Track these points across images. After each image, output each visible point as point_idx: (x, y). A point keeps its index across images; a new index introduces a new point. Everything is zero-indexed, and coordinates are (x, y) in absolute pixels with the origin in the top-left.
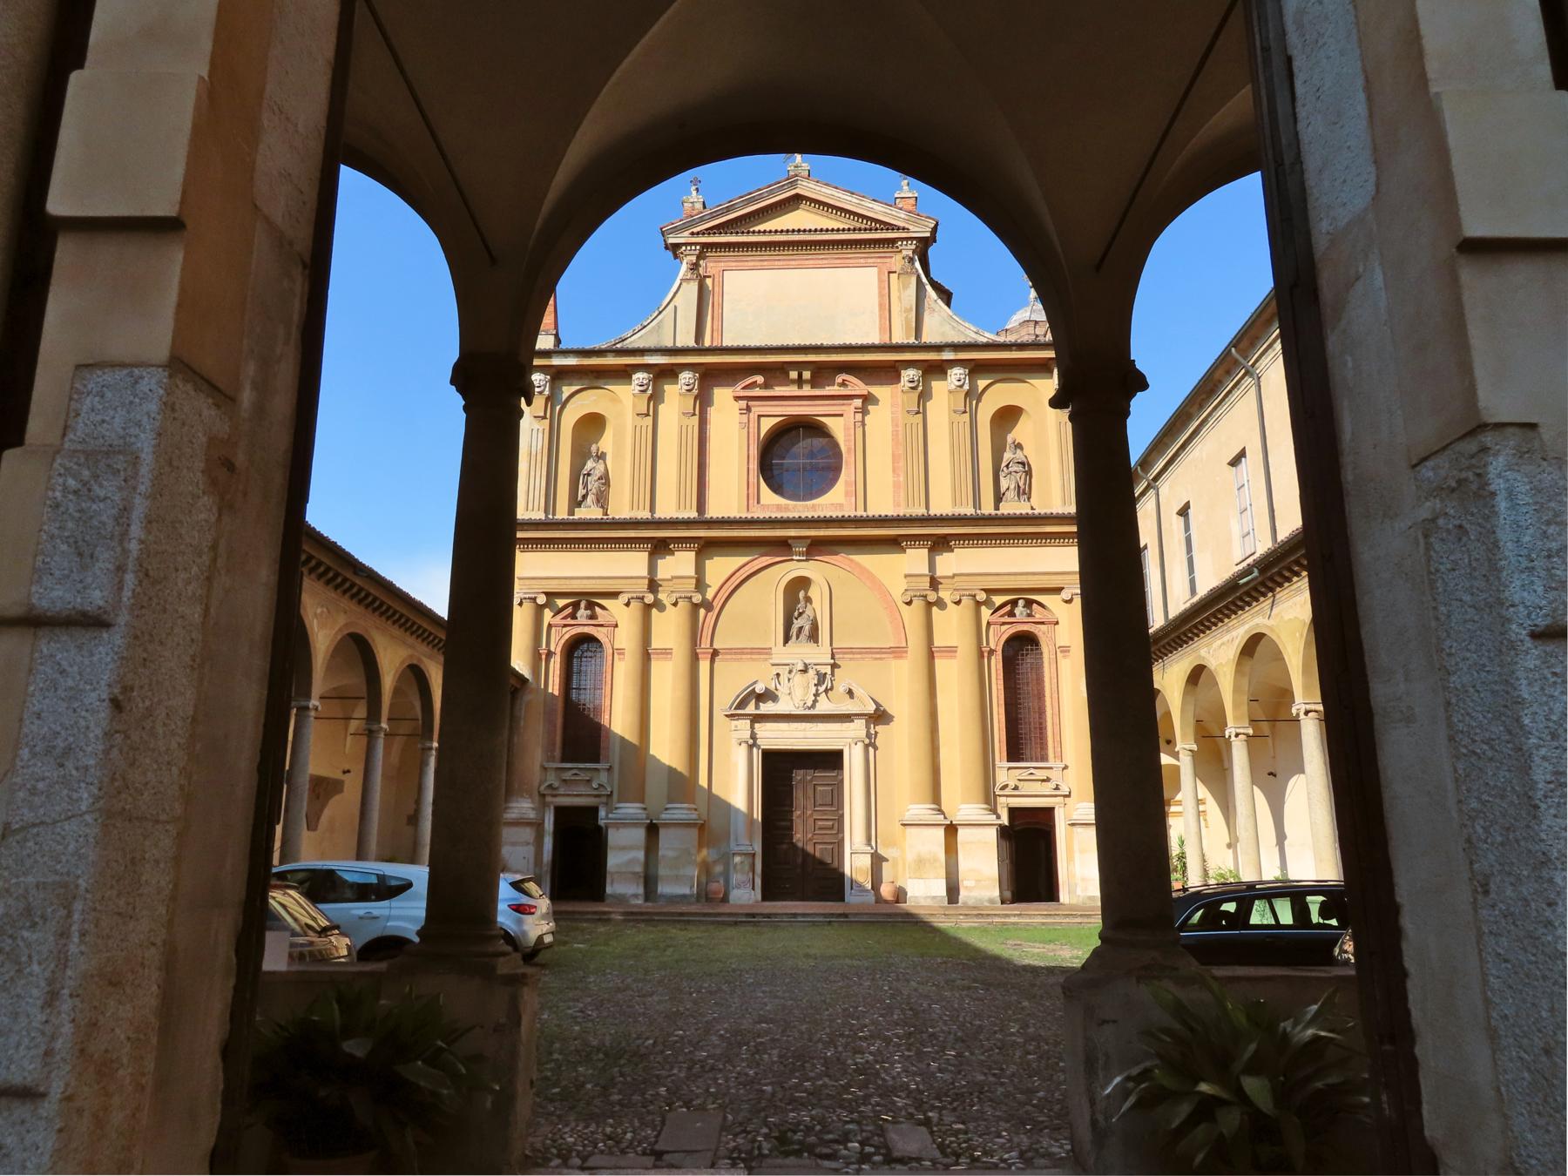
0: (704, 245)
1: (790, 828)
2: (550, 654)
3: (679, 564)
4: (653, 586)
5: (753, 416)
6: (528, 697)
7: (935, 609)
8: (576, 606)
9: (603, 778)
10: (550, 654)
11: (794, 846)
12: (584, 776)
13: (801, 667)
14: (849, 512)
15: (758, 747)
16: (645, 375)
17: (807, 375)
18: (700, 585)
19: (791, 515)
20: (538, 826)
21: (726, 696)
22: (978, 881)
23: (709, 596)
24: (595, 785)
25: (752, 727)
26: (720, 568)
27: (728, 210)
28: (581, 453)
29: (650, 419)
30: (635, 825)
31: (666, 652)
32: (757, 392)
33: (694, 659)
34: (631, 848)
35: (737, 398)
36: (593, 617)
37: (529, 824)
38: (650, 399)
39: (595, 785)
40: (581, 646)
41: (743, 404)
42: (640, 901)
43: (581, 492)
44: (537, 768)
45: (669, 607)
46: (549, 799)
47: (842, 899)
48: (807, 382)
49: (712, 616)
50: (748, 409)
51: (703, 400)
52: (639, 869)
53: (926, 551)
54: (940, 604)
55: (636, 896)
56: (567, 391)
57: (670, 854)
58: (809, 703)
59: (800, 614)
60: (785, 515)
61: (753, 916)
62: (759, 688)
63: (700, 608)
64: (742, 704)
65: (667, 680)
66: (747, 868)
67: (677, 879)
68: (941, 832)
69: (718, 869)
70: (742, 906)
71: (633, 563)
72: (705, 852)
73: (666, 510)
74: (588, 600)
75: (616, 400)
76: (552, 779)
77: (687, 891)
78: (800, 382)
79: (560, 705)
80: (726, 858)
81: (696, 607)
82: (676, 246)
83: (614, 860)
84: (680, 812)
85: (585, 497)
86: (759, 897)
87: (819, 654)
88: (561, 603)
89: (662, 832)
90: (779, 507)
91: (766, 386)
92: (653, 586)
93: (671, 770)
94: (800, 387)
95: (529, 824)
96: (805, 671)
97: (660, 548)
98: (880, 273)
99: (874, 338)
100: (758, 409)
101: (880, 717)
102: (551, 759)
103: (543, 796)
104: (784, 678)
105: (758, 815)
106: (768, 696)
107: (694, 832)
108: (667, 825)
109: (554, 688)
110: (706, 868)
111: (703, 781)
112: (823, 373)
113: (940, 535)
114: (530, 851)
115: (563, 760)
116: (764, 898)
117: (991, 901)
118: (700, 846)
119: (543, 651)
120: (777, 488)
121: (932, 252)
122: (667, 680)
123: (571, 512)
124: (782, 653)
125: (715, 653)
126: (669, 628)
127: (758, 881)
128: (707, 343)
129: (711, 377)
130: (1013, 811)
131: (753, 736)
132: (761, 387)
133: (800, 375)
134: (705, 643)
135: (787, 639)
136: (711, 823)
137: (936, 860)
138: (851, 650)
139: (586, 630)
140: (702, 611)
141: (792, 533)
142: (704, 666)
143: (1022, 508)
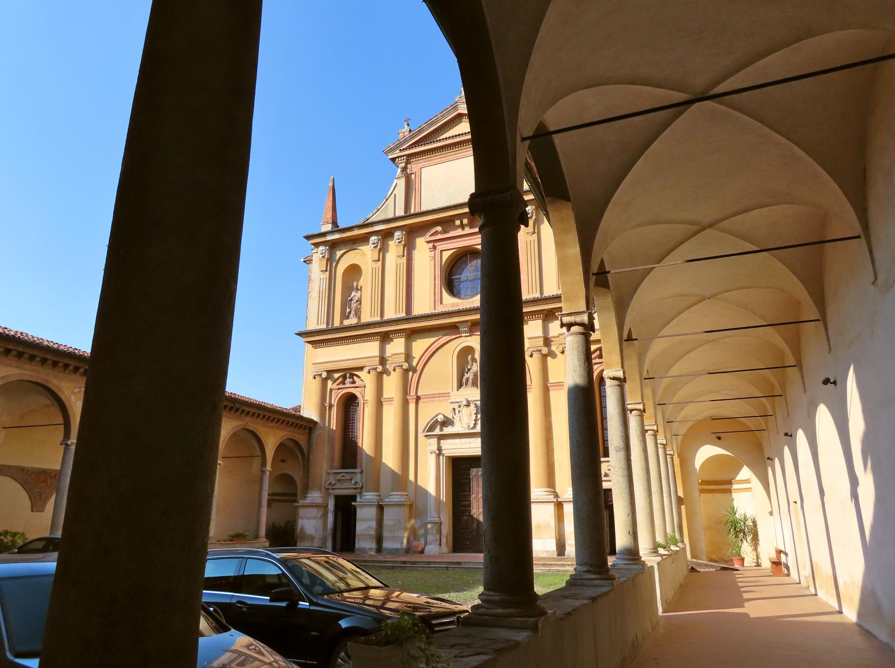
1: (469, 506)
2: (331, 406)
3: (397, 346)
4: (383, 360)
5: (438, 252)
6: (317, 432)
7: (549, 359)
8: (344, 377)
9: (358, 478)
10: (331, 406)
11: (472, 517)
12: (348, 477)
13: (465, 403)
15: (443, 455)
16: (376, 237)
17: (465, 221)
18: (408, 357)
20: (326, 507)
21: (423, 423)
23: (414, 364)
24: (353, 482)
25: (439, 443)
26: (420, 346)
27: (420, 132)
28: (348, 288)
29: (380, 262)
30: (370, 506)
31: (390, 400)
32: (439, 237)
33: (405, 403)
35: (428, 242)
36: (354, 382)
37: (317, 506)
38: (380, 250)
39: (353, 482)
40: (350, 402)
41: (431, 245)
42: (373, 553)
43: (348, 310)
44: (324, 473)
45: (392, 372)
46: (330, 491)
48: (466, 225)
49: (416, 376)
50: (434, 248)
51: (409, 247)
52: (373, 532)
54: (552, 354)
55: (371, 549)
56: (339, 253)
58: (472, 426)
59: (469, 370)
62: (440, 418)
63: (409, 371)
64: (431, 428)
65: (391, 415)
69: (422, 532)
71: (371, 349)
72: (413, 521)
73: (389, 314)
74: (349, 373)
75: (364, 254)
78: (462, 226)
79: (338, 438)
80: (425, 525)
81: (406, 371)
82: (393, 160)
83: (360, 527)
85: (350, 313)
86: (445, 549)
88: (336, 376)
89: (386, 509)
90: (453, 305)
91: (445, 231)
92: (383, 360)
93: (393, 471)
94: (463, 229)
95: (317, 506)
96: (468, 405)
97: (385, 338)
100: (440, 246)
102: (332, 467)
104: (457, 412)
105: (443, 497)
106: (447, 422)
107: (407, 510)
109: (334, 423)
110: (414, 533)
111: (412, 477)
115: (343, 467)
118: (410, 517)
119: (327, 405)
122: (391, 415)
123: (341, 322)
125: (418, 399)
126: (392, 385)
128: (412, 212)
129: (413, 232)
131: (440, 449)
132: (441, 233)
133: (462, 222)
134: (413, 393)
135: (460, 386)
136: (416, 503)
140: (411, 373)
141: (456, 319)
142: (412, 406)
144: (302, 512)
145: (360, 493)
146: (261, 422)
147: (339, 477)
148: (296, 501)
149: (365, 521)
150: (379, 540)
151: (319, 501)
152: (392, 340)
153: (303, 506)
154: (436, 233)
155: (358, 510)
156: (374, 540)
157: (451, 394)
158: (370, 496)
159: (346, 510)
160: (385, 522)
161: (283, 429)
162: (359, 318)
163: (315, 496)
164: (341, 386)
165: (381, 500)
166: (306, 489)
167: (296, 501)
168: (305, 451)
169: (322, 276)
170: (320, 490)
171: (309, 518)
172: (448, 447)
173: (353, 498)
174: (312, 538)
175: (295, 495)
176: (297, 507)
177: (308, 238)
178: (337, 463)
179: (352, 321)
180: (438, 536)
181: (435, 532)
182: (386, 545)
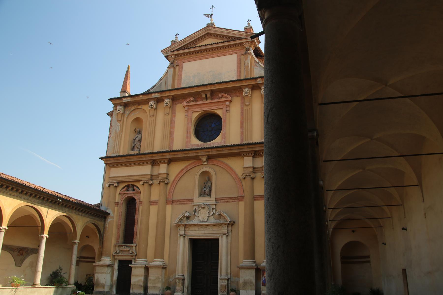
0: (176, 55)
12: (128, 249)
14: (223, 144)
17: (208, 95)
24: (130, 252)
26: (176, 169)
30: (141, 267)
34: (140, 276)
36: (134, 190)
37: (108, 266)
39: (130, 252)
41: (186, 108)
46: (116, 257)
58: (206, 220)
62: (187, 214)
64: (180, 221)
68: (253, 272)
76: (117, 249)
77: (157, 293)
78: (206, 98)
87: (211, 200)
89: (150, 270)
90: (198, 145)
91: (195, 100)
95: (108, 266)
97: (154, 163)
98: (238, 56)
101: (231, 224)
103: (115, 256)
104: (197, 211)
108: (151, 267)
112: (214, 94)
114: (108, 277)
124: (199, 201)
128: (176, 87)
132: (193, 101)
133: (206, 95)
137: (251, 282)
138: (223, 199)
139: (131, 195)
144: (98, 269)
145: (135, 259)
146: (74, 211)
147: (122, 248)
148: (94, 262)
149: (137, 277)
150: (146, 288)
151: (109, 263)
152: (159, 165)
153: (99, 266)
154: (190, 101)
155: (133, 269)
156: (142, 288)
157: (194, 200)
158: (141, 261)
159: (125, 268)
160: (149, 278)
161: (88, 217)
162: (139, 150)
163: (106, 260)
164: (126, 192)
165: (148, 264)
166: (101, 255)
167: (94, 262)
168: (102, 231)
169: (118, 124)
170: (110, 256)
171: (102, 273)
173: (130, 262)
174: (103, 286)
175: (94, 258)
176: (95, 266)
177: (110, 100)
178: (121, 240)
179: (136, 152)
180: (182, 287)
181: (181, 284)
182: (150, 291)
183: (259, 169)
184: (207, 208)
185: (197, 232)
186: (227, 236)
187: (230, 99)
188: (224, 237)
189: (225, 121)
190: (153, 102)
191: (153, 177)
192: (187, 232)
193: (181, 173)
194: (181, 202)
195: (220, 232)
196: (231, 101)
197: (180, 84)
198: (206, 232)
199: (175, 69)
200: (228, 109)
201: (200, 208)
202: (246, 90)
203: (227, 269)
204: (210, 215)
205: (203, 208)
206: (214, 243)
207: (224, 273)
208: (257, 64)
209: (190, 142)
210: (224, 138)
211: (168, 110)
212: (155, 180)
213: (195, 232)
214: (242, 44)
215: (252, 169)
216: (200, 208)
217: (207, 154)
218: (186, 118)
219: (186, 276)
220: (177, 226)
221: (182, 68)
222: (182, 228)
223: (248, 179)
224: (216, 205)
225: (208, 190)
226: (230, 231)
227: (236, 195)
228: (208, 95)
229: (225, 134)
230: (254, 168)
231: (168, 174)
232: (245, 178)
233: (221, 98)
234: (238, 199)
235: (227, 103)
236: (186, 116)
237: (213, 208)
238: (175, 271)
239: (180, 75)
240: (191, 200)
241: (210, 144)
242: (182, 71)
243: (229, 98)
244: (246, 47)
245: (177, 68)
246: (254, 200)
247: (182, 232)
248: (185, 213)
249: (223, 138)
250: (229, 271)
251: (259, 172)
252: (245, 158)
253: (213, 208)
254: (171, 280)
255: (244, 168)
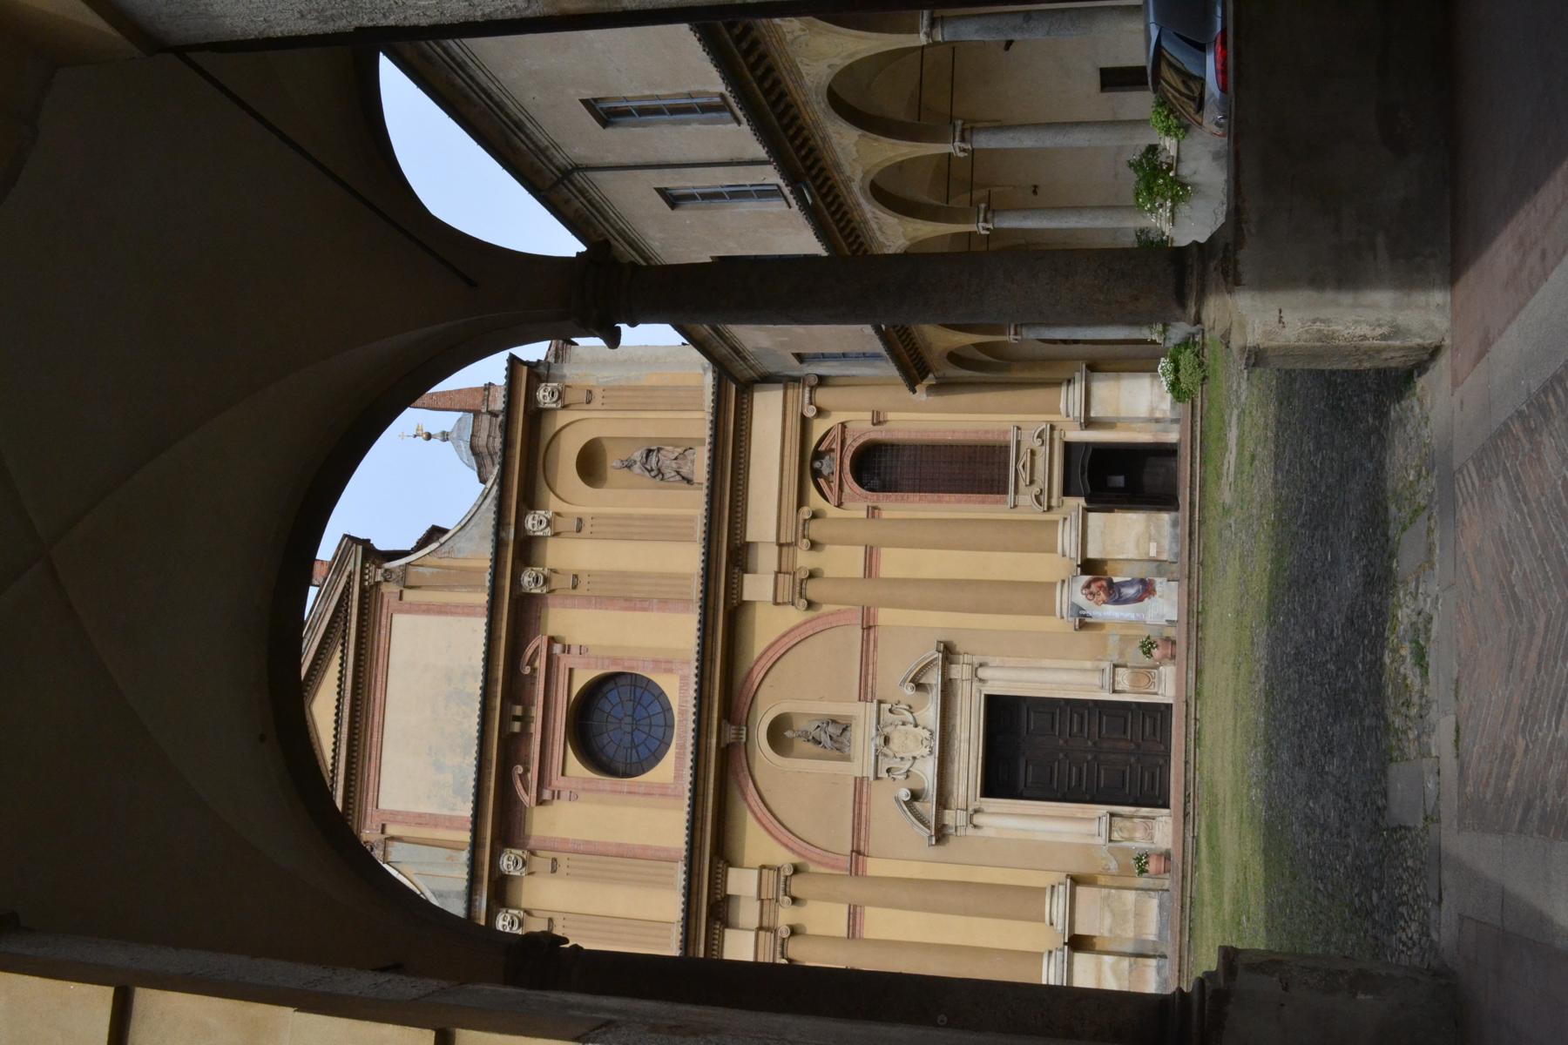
17: (518, 710)
19: (690, 741)
22: (1150, 539)
41: (547, 795)
47: (1169, 707)
52: (1126, 962)
53: (746, 576)
55: (1159, 970)
57: (1108, 921)
58: (927, 734)
60: (690, 749)
61: (1186, 815)
62: (904, 794)
66: (1128, 824)
67: (1139, 915)
70: (1175, 832)
78: (525, 720)
84: (1057, 908)
86: (1165, 811)
87: (863, 716)
89: (1079, 930)
90: (680, 757)
98: (401, 611)
99: (481, 623)
107: (1081, 891)
113: (727, 554)
116: (1166, 806)
117: (1175, 524)
120: (655, 757)
121: (381, 545)
124: (861, 762)
127: (1144, 811)
130: (1067, 491)
132: (526, 770)
133: (517, 718)
135: (847, 759)
143: (702, 457)
154: (523, 777)
157: (859, 775)
172: (962, 790)
183: (784, 559)
184: (887, 730)
185: (963, 765)
186: (981, 665)
187: (545, 639)
188: (982, 673)
189: (615, 661)
190: (500, 917)
191: (765, 924)
192: (961, 802)
193: (765, 821)
194: (859, 824)
195: (966, 685)
196: (552, 640)
197: (451, 822)
198: (964, 736)
199: (393, 838)
200: (575, 650)
201: (885, 750)
202: (527, 579)
203: (1085, 670)
204: (911, 719)
205: (887, 740)
206: (1000, 710)
207: (1096, 679)
208: (445, 548)
209: (663, 786)
210: (667, 666)
211: (541, 863)
212: (776, 916)
213: (963, 774)
214: (363, 590)
215: (781, 576)
216: (885, 750)
217: (715, 715)
218: (582, 795)
219: (1103, 810)
220: (941, 834)
221: (394, 813)
222: (949, 817)
223: (813, 590)
224: (880, 702)
225: (831, 729)
226: (967, 658)
227: (858, 632)
228: (518, 710)
229: (656, 662)
230: (779, 572)
231: (763, 867)
232: (811, 605)
233: (534, 670)
234: (869, 628)
235: (557, 649)
236: (573, 797)
237: (891, 711)
238: (1086, 849)
239: (422, 820)
240: (859, 783)
241: (682, 712)
242: (407, 814)
243: (540, 642)
244: (379, 578)
245: (392, 830)
246: (877, 577)
247: (961, 818)
248: (897, 800)
249: (670, 671)
250: (1088, 664)
251: (794, 556)
252: (746, 598)
253: (891, 711)
254: (1113, 865)
255: (776, 603)
